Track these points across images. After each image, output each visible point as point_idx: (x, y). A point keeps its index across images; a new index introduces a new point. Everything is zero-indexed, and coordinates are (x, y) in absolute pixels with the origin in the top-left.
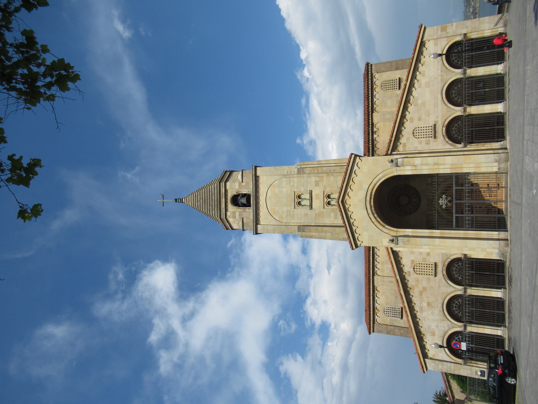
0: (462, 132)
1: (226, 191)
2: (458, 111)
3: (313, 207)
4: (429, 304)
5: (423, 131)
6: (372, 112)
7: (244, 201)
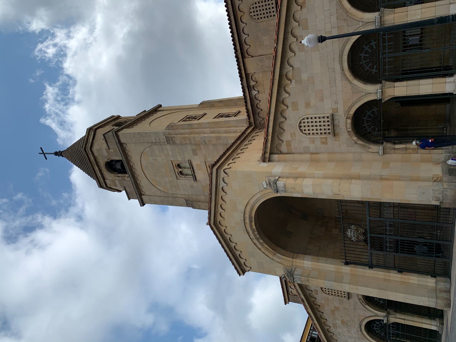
2: (371, 92)
3: (198, 178)
4: (343, 322)
5: (314, 124)
6: (243, 57)
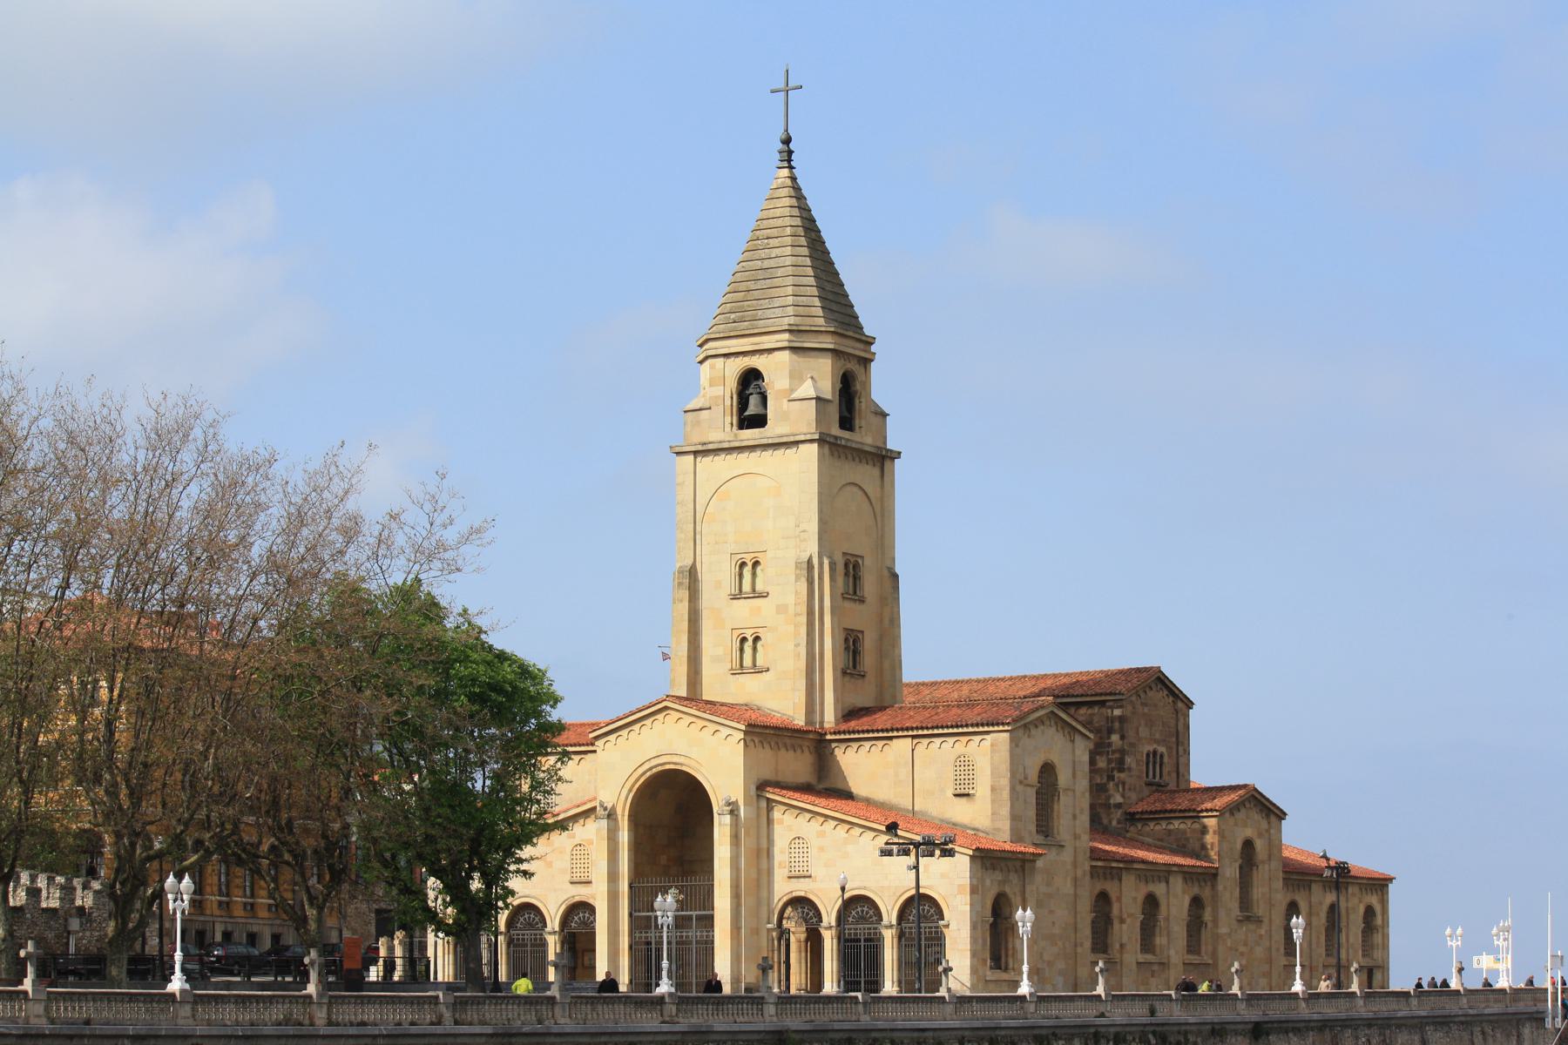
7: (753, 408)
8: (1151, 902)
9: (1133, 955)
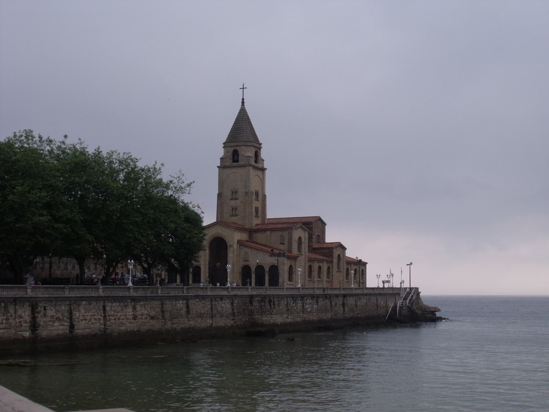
0: (246, 272)
1: (240, 146)
2: (253, 270)
7: (235, 158)
8: (320, 268)
9: (316, 279)
